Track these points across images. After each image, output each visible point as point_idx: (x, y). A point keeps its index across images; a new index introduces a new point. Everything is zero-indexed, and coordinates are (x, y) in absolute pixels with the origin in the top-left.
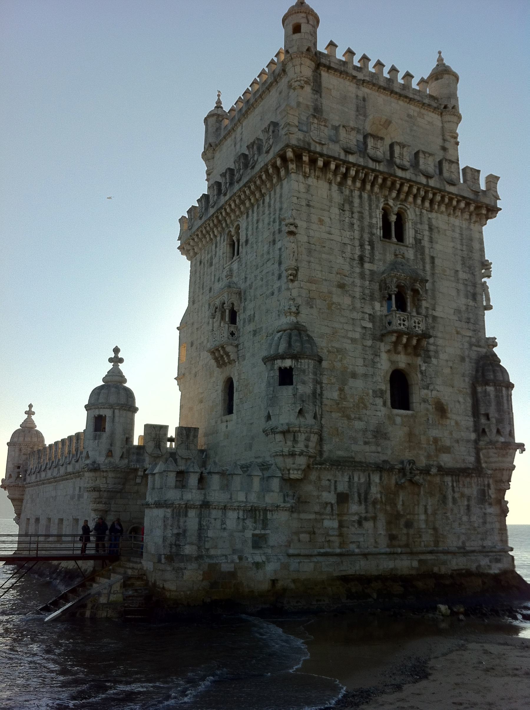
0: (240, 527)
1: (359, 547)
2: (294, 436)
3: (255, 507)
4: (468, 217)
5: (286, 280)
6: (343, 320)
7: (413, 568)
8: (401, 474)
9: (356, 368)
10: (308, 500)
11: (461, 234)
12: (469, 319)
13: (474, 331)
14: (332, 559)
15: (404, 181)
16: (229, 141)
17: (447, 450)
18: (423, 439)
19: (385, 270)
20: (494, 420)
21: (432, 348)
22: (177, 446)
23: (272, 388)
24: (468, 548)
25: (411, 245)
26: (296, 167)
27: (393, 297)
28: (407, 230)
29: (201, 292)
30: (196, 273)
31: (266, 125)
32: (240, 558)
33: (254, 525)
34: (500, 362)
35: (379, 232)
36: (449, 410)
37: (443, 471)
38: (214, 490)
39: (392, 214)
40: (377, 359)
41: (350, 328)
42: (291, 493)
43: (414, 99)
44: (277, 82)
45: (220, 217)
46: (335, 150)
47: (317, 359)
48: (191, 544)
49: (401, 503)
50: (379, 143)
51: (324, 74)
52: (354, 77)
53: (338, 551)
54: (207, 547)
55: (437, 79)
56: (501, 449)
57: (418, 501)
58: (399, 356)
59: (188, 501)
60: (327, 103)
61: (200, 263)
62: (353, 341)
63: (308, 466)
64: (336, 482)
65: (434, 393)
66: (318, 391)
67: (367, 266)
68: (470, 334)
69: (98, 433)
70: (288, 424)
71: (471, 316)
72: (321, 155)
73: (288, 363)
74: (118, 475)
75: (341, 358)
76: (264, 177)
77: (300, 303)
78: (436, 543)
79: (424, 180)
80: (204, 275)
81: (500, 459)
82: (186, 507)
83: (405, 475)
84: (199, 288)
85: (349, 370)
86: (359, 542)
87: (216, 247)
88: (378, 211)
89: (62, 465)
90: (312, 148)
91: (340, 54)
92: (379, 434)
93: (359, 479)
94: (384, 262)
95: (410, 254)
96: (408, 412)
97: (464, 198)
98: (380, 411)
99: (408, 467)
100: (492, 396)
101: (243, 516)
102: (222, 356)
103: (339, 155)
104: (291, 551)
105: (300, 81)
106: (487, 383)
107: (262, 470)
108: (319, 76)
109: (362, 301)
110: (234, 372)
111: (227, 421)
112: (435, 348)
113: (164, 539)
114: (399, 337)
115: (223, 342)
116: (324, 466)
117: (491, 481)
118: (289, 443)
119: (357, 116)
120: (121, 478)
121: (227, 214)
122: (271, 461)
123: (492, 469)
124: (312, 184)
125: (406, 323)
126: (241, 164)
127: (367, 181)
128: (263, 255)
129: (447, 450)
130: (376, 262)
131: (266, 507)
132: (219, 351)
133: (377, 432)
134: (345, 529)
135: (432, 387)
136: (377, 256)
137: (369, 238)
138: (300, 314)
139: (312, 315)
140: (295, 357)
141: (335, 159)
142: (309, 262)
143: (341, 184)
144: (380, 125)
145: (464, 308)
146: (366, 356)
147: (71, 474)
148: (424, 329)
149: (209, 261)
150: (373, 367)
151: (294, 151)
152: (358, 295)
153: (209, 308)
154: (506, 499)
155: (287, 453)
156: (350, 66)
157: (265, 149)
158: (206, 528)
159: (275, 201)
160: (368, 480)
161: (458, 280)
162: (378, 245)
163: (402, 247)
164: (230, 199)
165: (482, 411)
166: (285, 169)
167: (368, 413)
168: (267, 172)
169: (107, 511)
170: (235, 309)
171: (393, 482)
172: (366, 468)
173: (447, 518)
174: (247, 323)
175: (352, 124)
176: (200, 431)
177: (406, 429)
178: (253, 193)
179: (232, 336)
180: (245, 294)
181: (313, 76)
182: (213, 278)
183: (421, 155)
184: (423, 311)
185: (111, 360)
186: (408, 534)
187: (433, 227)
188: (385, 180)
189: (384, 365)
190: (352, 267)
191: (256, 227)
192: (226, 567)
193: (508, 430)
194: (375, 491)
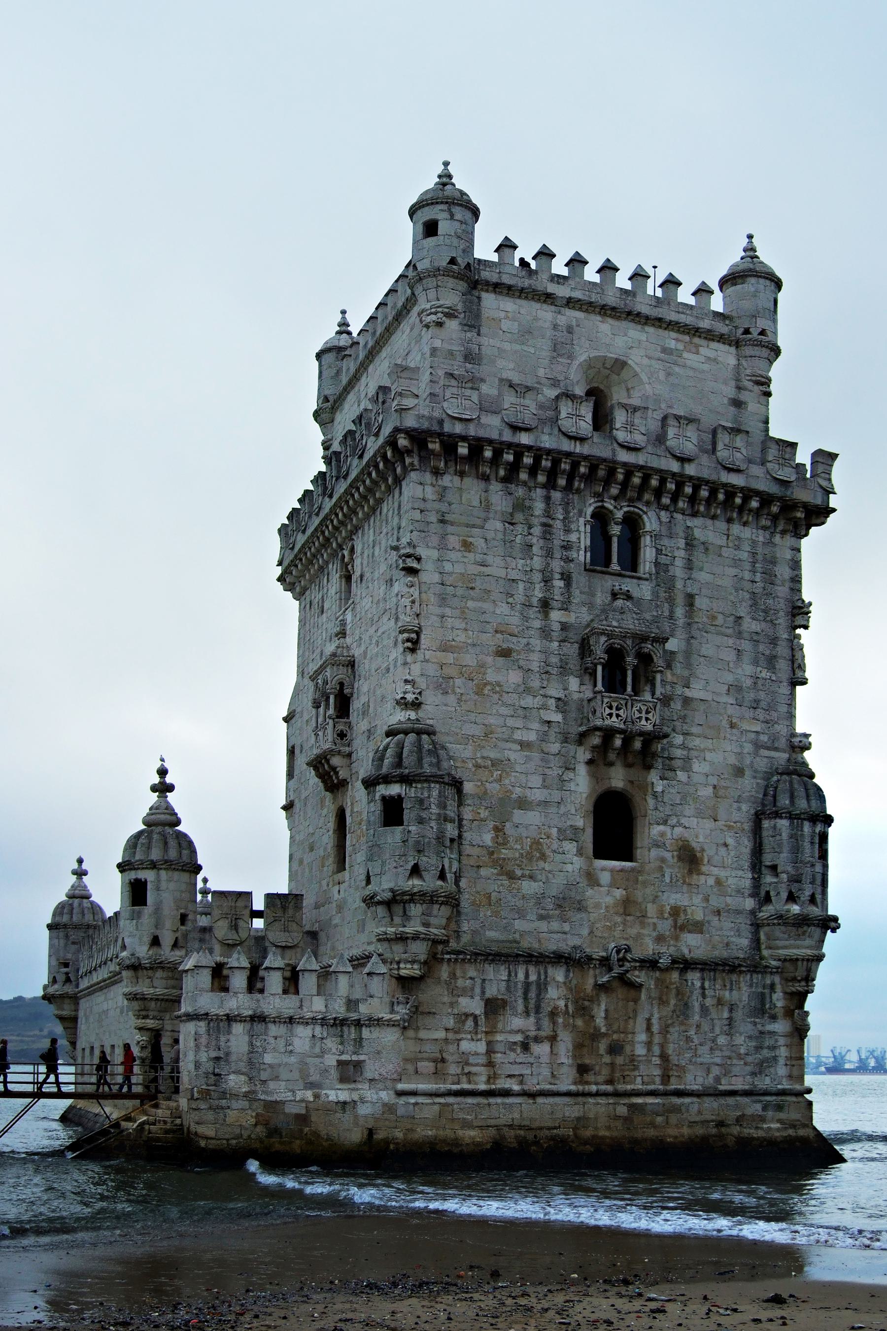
1: (521, 1083)
6: (504, 711)
9: (528, 791)
14: (470, 1100)
17: (698, 927)
18: (651, 910)
19: (592, 621)
21: (678, 753)
23: (372, 831)
24: (721, 1088)
26: (420, 461)
27: (599, 669)
35: (582, 556)
36: (706, 860)
37: (684, 965)
40: (571, 775)
41: (519, 723)
46: (492, 427)
47: (446, 780)
49: (603, 1015)
53: (483, 1087)
56: (794, 925)
57: (635, 1011)
58: (613, 769)
62: (525, 745)
64: (484, 980)
65: (678, 830)
67: (556, 616)
75: (500, 775)
81: (792, 942)
85: (514, 796)
92: (567, 904)
93: (527, 976)
94: (591, 606)
109: (544, 676)
112: (685, 753)
116: (461, 957)
117: (777, 979)
123: (779, 960)
125: (621, 712)
129: (698, 927)
130: (573, 607)
134: (499, 1055)
135: (675, 821)
136: (577, 596)
138: (423, 706)
139: (446, 705)
140: (405, 780)
141: (490, 442)
146: (549, 772)
150: (561, 789)
152: (535, 666)
154: (805, 1009)
160: (543, 977)
165: (768, 859)
170: (346, 691)
171: (591, 981)
173: (688, 1039)
177: (619, 893)
179: (342, 739)
186: (612, 1065)
189: (582, 785)
190: (526, 619)
194: (555, 995)
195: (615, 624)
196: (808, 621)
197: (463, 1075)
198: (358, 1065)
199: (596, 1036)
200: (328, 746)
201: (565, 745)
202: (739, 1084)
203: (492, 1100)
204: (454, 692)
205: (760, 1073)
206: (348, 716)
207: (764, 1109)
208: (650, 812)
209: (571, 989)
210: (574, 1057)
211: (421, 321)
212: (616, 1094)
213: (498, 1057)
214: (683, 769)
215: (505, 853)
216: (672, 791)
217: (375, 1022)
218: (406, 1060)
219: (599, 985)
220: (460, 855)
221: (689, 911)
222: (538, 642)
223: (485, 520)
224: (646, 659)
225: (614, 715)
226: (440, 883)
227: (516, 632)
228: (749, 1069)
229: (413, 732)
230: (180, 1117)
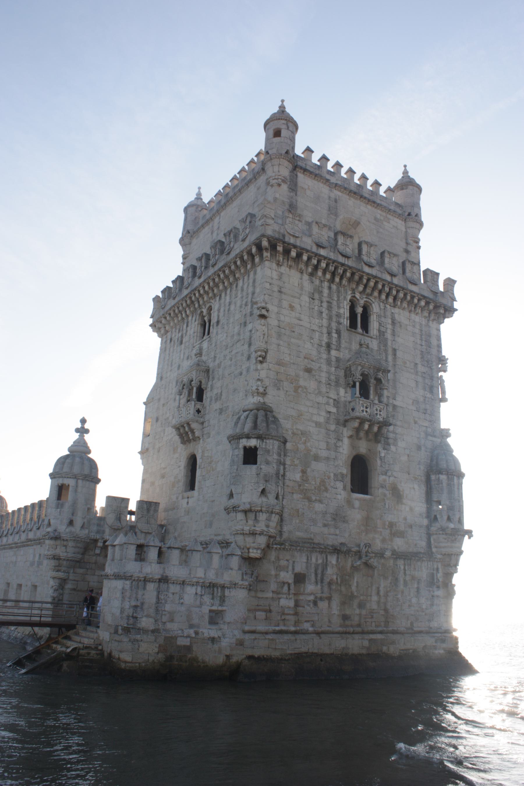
0: (198, 603)
1: (313, 626)
2: (256, 515)
3: (213, 584)
4: (427, 315)
5: (255, 361)
10: (266, 579)
11: (421, 330)
12: (426, 410)
13: (430, 421)
14: (286, 637)
16: (207, 229)
17: (401, 534)
19: (350, 358)
21: (391, 435)
23: (235, 467)
24: (415, 629)
25: (375, 337)
26: (271, 256)
27: (358, 384)
28: (372, 323)
30: (165, 350)
31: (244, 215)
32: (197, 633)
33: (211, 601)
35: (346, 322)
36: (405, 497)
37: (397, 555)
38: (174, 565)
39: (358, 306)
40: (340, 444)
41: (315, 411)
42: (249, 572)
43: (381, 205)
44: (256, 179)
45: (193, 298)
46: (307, 243)
47: (282, 440)
48: (148, 616)
49: (355, 584)
50: (348, 241)
51: (301, 176)
52: (328, 180)
53: (293, 629)
54: (164, 620)
55: (402, 189)
56: (451, 535)
59: (147, 574)
60: (301, 201)
61: (171, 341)
62: (318, 424)
63: (268, 546)
64: (294, 562)
65: (392, 479)
66: (282, 472)
67: (333, 353)
68: (426, 424)
70: (250, 503)
72: (295, 247)
73: (253, 443)
74: (78, 545)
75: (305, 440)
76: (239, 263)
77: (267, 384)
78: (387, 623)
79: (388, 278)
80: (173, 352)
82: (144, 580)
83: (360, 558)
84: (168, 364)
85: (312, 453)
87: (187, 326)
89: (24, 532)
90: (287, 239)
91: (315, 159)
92: (338, 517)
93: (317, 560)
94: (350, 350)
95: (374, 344)
96: (366, 496)
97: (425, 297)
98: (340, 492)
99: (364, 550)
100: (445, 485)
101: (201, 592)
102: (187, 433)
103: (311, 248)
104: (247, 628)
105: (277, 179)
106: (440, 472)
107: (222, 548)
108: (295, 176)
109: (328, 386)
111: (188, 498)
112: (394, 435)
113: (122, 612)
114: (362, 423)
115: (188, 419)
116: (283, 547)
118: (250, 522)
119: (329, 214)
120: (81, 548)
121: (201, 295)
122: (231, 539)
123: (442, 554)
124: (284, 272)
125: (368, 410)
126: (217, 250)
127: (336, 273)
129: (401, 534)
130: (342, 350)
131: (224, 584)
132: (184, 427)
133: (336, 515)
135: (390, 473)
136: (344, 344)
137: (337, 327)
139: (279, 396)
140: (259, 437)
141: (307, 251)
142: (279, 345)
143: (311, 275)
144: (350, 225)
145: (422, 399)
146: (329, 440)
147: (31, 541)
148: (385, 417)
149: (180, 339)
151: (269, 241)
152: (324, 380)
153: (177, 384)
155: (248, 532)
156: (324, 171)
157: (241, 237)
158: (163, 602)
159: (248, 285)
160: (325, 561)
161: (417, 372)
163: (366, 338)
164: (204, 281)
166: (260, 256)
167: (328, 495)
168: (242, 258)
169: (65, 580)
170: (202, 387)
171: (349, 564)
172: (324, 550)
174: (213, 401)
175: (323, 221)
178: (227, 277)
179: (198, 413)
180: (213, 372)
181: (290, 176)
183: (386, 255)
184: (385, 400)
185: (77, 430)
186: (360, 615)
187: (395, 322)
188: (353, 274)
189: (345, 450)
190: (319, 353)
191: (228, 308)
192: (182, 642)
193: (457, 517)
194: (331, 572)
199: (352, 597)
200: (191, 416)
201: (338, 426)
203: (298, 637)
204: (283, 390)
206: (202, 402)
207: (436, 642)
208: (378, 468)
216: (388, 456)
217: (234, 585)
218: (249, 610)
222: (325, 366)
223: (301, 295)
226: (276, 501)
227: (314, 359)
229: (262, 409)
230: (100, 645)
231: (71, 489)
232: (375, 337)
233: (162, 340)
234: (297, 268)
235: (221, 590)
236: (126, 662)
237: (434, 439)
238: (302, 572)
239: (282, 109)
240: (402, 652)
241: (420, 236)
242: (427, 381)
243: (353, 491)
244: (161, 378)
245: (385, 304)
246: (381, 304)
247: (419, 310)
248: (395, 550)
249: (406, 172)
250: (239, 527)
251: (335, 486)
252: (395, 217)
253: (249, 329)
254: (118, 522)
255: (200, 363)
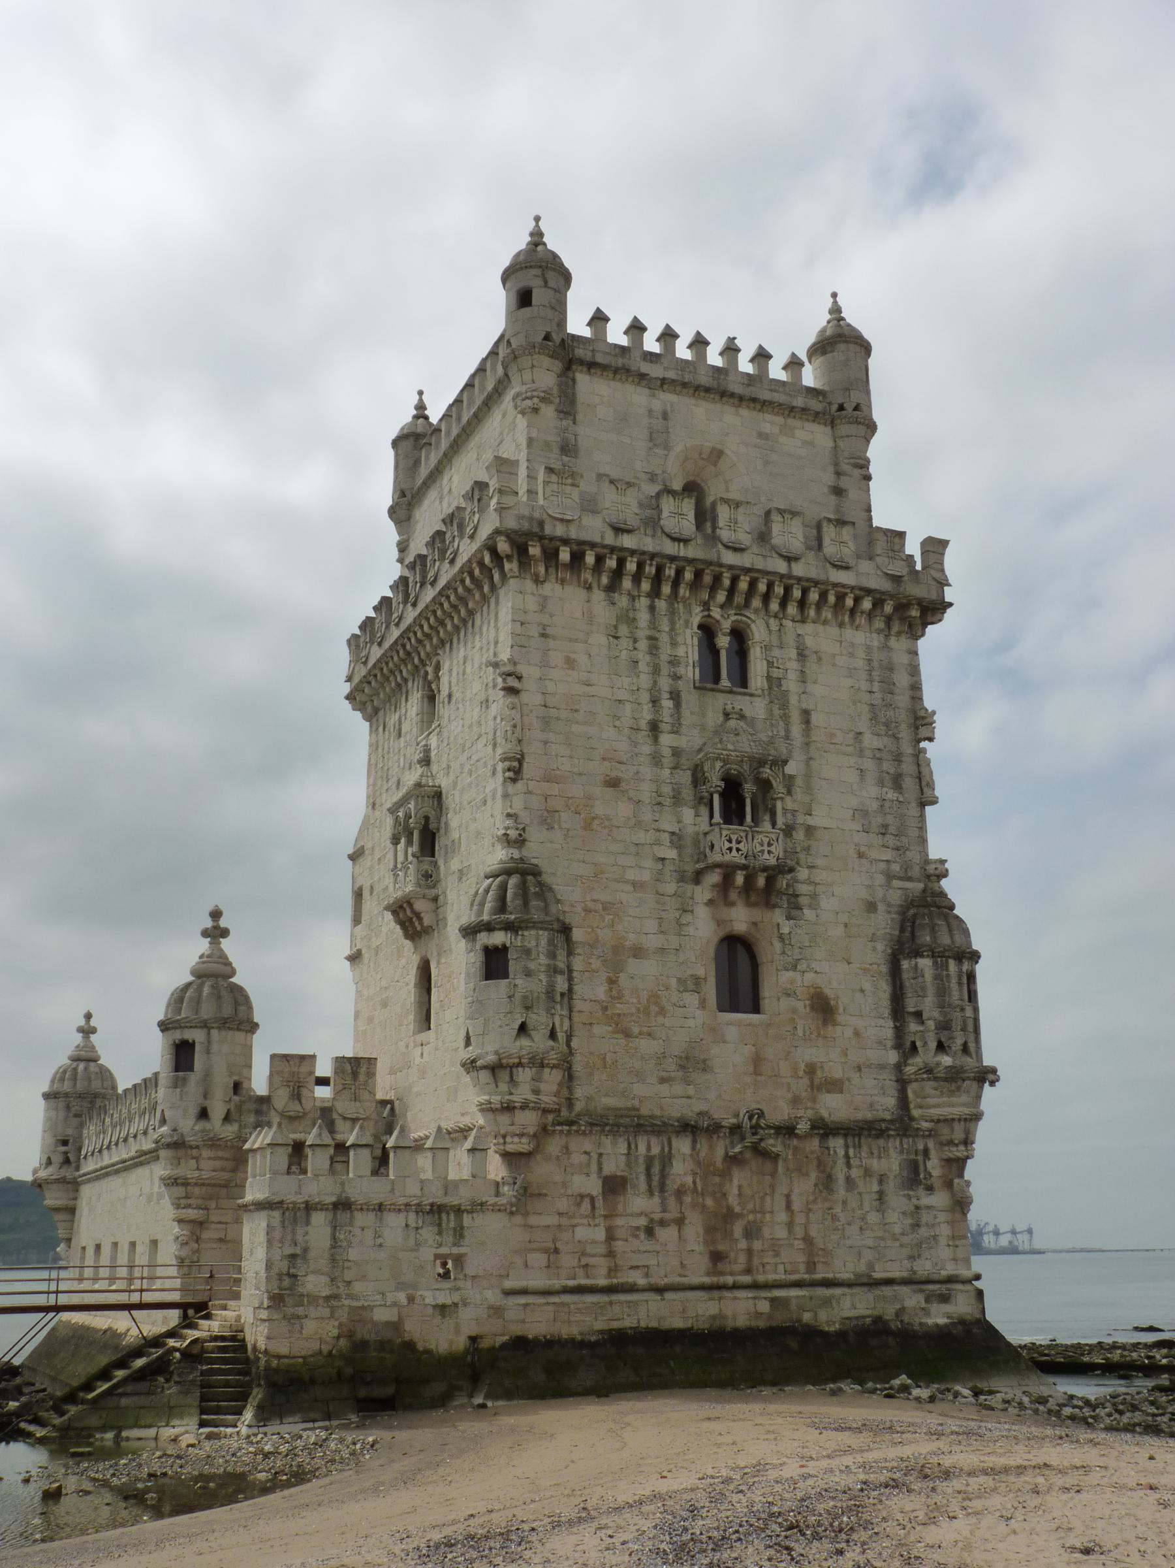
0: (411, 1242)
1: (647, 1275)
7: (758, 1315)
8: (736, 1138)
12: (886, 826)
13: (897, 849)
14: (590, 1298)
15: (738, 572)
17: (835, 1086)
19: (705, 744)
20: (931, 1024)
21: (803, 889)
22: (337, 1093)
25: (760, 692)
29: (385, 787)
31: (468, 487)
32: (411, 1299)
34: (952, 907)
35: (691, 672)
37: (824, 1129)
40: (688, 918)
43: (771, 403)
45: (408, 647)
46: (593, 529)
48: (316, 1272)
52: (642, 376)
53: (603, 1282)
54: (347, 1278)
56: (946, 1080)
57: (773, 1187)
58: (734, 909)
62: (637, 885)
63: (544, 1129)
64: (600, 1155)
65: (809, 976)
66: (561, 984)
67: (666, 740)
68: (888, 855)
69: (180, 1074)
70: (497, 1053)
71: (890, 819)
72: (566, 542)
73: (498, 938)
74: (220, 1154)
76: (468, 581)
79: (781, 567)
81: (945, 1099)
85: (627, 943)
86: (647, 1267)
88: (688, 632)
90: (548, 530)
91: (616, 335)
92: (692, 1063)
93: (649, 1148)
94: (703, 728)
96: (751, 1016)
97: (869, 592)
98: (695, 1016)
99: (747, 1124)
104: (508, 1284)
106: (918, 954)
109: (656, 808)
110: (431, 947)
112: (811, 888)
113: (268, 1267)
116: (574, 1128)
118: (503, 1087)
120: (227, 1159)
121: (419, 641)
123: (932, 1121)
125: (741, 846)
128: (471, 726)
129: (835, 1086)
130: (684, 729)
131: (460, 1205)
133: (687, 1058)
134: (620, 1243)
135: (804, 966)
136: (687, 718)
140: (509, 927)
141: (593, 545)
145: (875, 805)
146: (663, 915)
152: (646, 797)
155: (498, 1106)
156: (636, 355)
158: (345, 1244)
160: (666, 1149)
161: (861, 751)
162: (690, 698)
165: (911, 1005)
167: (667, 1022)
168: (471, 574)
169: (201, 1223)
170: (432, 826)
171: (720, 1152)
173: (834, 1218)
176: (379, 1065)
177: (748, 1050)
181: (559, 385)
182: (402, 760)
183: (776, 517)
185: (205, 933)
187: (805, 652)
188: (698, 574)
189: (703, 930)
190: (635, 744)
192: (382, 1315)
193: (959, 1041)
194: (681, 1171)
195: (730, 747)
196: (933, 732)
197: (579, 1267)
198: (459, 1260)
199: (729, 1216)
202: (897, 1273)
203: (614, 1297)
204: (560, 828)
205: (919, 1256)
209: (699, 1163)
210: (706, 1242)
211: (516, 407)
212: (755, 1286)
213: (619, 1246)
214: (811, 907)
215: (620, 1008)
219: (731, 1157)
220: (571, 1011)
221: (826, 1068)
224: (765, 785)
225: (734, 850)
226: (551, 1043)
228: (906, 1251)
231: (197, 1048)
232: (760, 692)
233: (371, 726)
234: (579, 581)
235: (455, 1216)
236: (279, 1357)
237: (907, 885)
238: (619, 1174)
239: (536, 239)
240: (848, 1322)
241: (870, 454)
242: (886, 766)
243: (721, 1009)
244: (374, 805)
245: (780, 619)
246: (772, 620)
247: (861, 620)
248: (823, 1119)
249: (836, 310)
250: (484, 1098)
251: (681, 1003)
252: (808, 420)
253: (493, 714)
254: (297, 1102)
255: (424, 781)
